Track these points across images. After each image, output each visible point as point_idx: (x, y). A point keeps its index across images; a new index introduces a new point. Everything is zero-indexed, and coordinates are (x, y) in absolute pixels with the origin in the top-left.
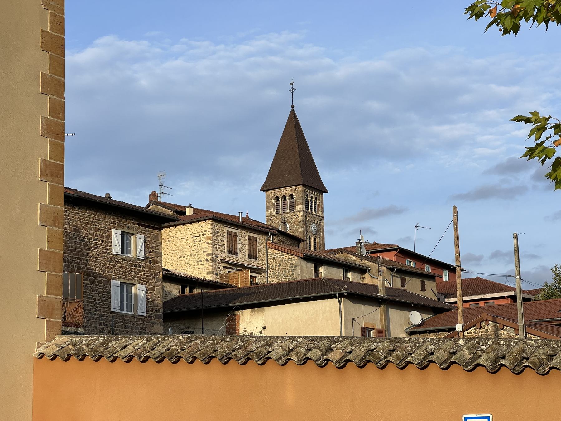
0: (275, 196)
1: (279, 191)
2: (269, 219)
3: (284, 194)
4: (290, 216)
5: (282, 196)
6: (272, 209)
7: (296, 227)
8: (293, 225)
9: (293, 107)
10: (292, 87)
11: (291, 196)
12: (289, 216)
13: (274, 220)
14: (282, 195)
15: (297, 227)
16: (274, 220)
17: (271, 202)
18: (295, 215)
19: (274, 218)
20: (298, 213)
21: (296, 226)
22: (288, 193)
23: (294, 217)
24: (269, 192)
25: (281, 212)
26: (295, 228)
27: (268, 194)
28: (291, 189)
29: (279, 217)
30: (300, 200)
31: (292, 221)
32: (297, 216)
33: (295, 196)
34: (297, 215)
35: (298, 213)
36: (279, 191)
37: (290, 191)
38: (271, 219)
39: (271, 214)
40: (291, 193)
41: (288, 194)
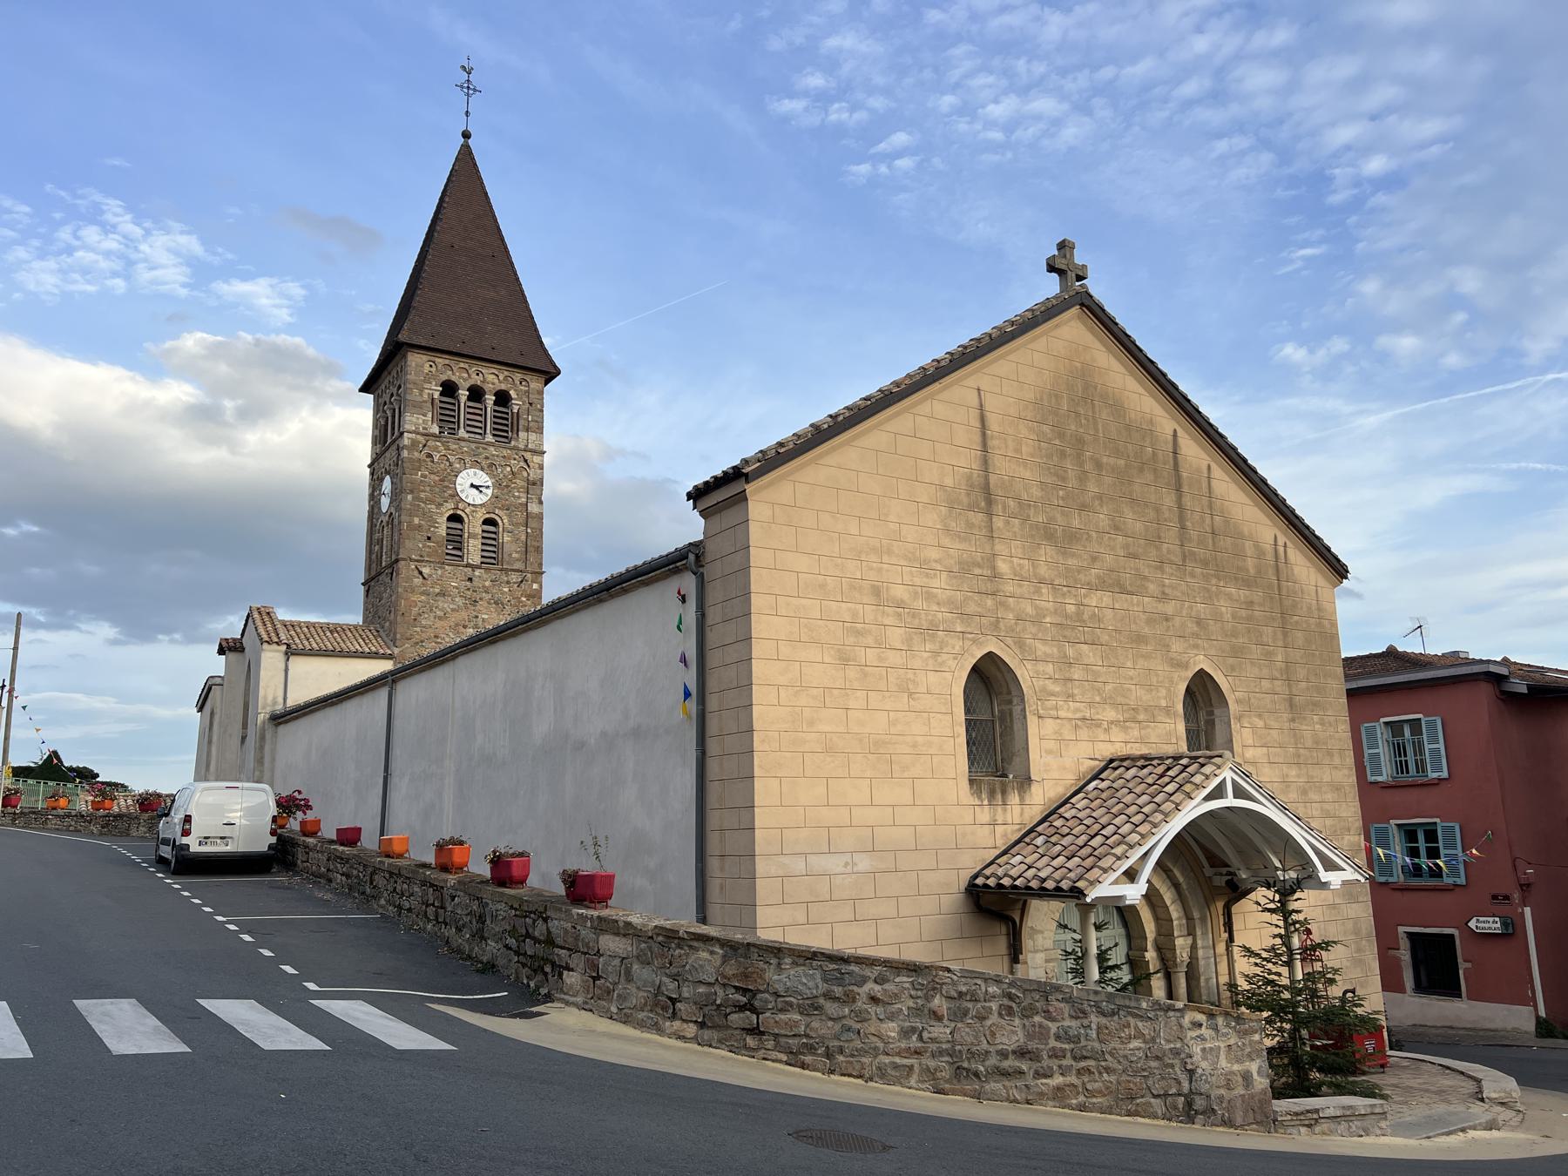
0: (444, 378)
1: (462, 365)
2: (420, 442)
3: (477, 380)
4: (497, 456)
5: (467, 385)
6: (430, 415)
7: (516, 494)
8: (507, 486)
9: (466, 135)
10: (468, 81)
11: (503, 398)
12: (493, 455)
13: (436, 449)
14: (471, 382)
15: (519, 497)
16: (436, 449)
17: (426, 391)
18: (517, 457)
19: (438, 444)
20: (528, 455)
21: (518, 492)
22: (493, 384)
23: (513, 462)
24: (425, 358)
25: (462, 433)
26: (514, 496)
27: (419, 360)
28: (506, 373)
29: (456, 446)
30: (535, 418)
31: (502, 472)
32: (522, 464)
33: (515, 399)
34: (526, 461)
35: (528, 455)
36: (462, 365)
37: (501, 378)
38: (425, 446)
39: (424, 428)
40: (503, 387)
41: (490, 385)
